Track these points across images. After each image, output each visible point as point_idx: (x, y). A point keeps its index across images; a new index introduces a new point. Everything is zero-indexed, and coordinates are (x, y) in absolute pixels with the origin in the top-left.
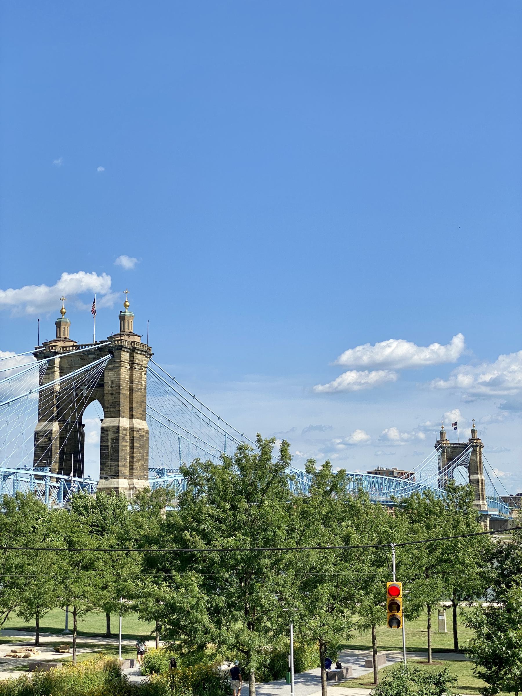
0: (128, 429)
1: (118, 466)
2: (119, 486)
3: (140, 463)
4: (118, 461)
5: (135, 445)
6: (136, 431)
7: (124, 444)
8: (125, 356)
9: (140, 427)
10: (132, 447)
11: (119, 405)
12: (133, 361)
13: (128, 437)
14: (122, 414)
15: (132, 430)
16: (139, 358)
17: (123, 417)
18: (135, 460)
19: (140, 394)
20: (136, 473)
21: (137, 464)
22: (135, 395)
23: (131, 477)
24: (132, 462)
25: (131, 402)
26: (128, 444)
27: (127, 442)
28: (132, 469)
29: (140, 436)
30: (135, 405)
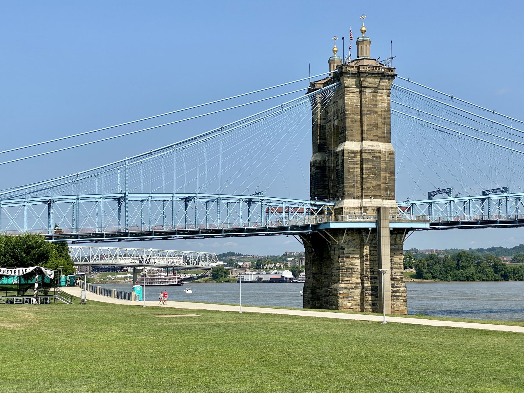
1: (344, 186)
2: (344, 206)
3: (374, 184)
4: (344, 183)
5: (364, 166)
7: (351, 166)
8: (350, 82)
9: (373, 148)
10: (362, 169)
11: (345, 130)
13: (358, 159)
14: (350, 138)
15: (362, 152)
16: (369, 81)
17: (352, 141)
18: (364, 180)
19: (373, 116)
20: (365, 193)
21: (369, 184)
22: (365, 118)
23: (362, 197)
24: (362, 183)
25: (362, 126)
26: (359, 166)
28: (362, 189)
29: (373, 157)
30: (364, 128)
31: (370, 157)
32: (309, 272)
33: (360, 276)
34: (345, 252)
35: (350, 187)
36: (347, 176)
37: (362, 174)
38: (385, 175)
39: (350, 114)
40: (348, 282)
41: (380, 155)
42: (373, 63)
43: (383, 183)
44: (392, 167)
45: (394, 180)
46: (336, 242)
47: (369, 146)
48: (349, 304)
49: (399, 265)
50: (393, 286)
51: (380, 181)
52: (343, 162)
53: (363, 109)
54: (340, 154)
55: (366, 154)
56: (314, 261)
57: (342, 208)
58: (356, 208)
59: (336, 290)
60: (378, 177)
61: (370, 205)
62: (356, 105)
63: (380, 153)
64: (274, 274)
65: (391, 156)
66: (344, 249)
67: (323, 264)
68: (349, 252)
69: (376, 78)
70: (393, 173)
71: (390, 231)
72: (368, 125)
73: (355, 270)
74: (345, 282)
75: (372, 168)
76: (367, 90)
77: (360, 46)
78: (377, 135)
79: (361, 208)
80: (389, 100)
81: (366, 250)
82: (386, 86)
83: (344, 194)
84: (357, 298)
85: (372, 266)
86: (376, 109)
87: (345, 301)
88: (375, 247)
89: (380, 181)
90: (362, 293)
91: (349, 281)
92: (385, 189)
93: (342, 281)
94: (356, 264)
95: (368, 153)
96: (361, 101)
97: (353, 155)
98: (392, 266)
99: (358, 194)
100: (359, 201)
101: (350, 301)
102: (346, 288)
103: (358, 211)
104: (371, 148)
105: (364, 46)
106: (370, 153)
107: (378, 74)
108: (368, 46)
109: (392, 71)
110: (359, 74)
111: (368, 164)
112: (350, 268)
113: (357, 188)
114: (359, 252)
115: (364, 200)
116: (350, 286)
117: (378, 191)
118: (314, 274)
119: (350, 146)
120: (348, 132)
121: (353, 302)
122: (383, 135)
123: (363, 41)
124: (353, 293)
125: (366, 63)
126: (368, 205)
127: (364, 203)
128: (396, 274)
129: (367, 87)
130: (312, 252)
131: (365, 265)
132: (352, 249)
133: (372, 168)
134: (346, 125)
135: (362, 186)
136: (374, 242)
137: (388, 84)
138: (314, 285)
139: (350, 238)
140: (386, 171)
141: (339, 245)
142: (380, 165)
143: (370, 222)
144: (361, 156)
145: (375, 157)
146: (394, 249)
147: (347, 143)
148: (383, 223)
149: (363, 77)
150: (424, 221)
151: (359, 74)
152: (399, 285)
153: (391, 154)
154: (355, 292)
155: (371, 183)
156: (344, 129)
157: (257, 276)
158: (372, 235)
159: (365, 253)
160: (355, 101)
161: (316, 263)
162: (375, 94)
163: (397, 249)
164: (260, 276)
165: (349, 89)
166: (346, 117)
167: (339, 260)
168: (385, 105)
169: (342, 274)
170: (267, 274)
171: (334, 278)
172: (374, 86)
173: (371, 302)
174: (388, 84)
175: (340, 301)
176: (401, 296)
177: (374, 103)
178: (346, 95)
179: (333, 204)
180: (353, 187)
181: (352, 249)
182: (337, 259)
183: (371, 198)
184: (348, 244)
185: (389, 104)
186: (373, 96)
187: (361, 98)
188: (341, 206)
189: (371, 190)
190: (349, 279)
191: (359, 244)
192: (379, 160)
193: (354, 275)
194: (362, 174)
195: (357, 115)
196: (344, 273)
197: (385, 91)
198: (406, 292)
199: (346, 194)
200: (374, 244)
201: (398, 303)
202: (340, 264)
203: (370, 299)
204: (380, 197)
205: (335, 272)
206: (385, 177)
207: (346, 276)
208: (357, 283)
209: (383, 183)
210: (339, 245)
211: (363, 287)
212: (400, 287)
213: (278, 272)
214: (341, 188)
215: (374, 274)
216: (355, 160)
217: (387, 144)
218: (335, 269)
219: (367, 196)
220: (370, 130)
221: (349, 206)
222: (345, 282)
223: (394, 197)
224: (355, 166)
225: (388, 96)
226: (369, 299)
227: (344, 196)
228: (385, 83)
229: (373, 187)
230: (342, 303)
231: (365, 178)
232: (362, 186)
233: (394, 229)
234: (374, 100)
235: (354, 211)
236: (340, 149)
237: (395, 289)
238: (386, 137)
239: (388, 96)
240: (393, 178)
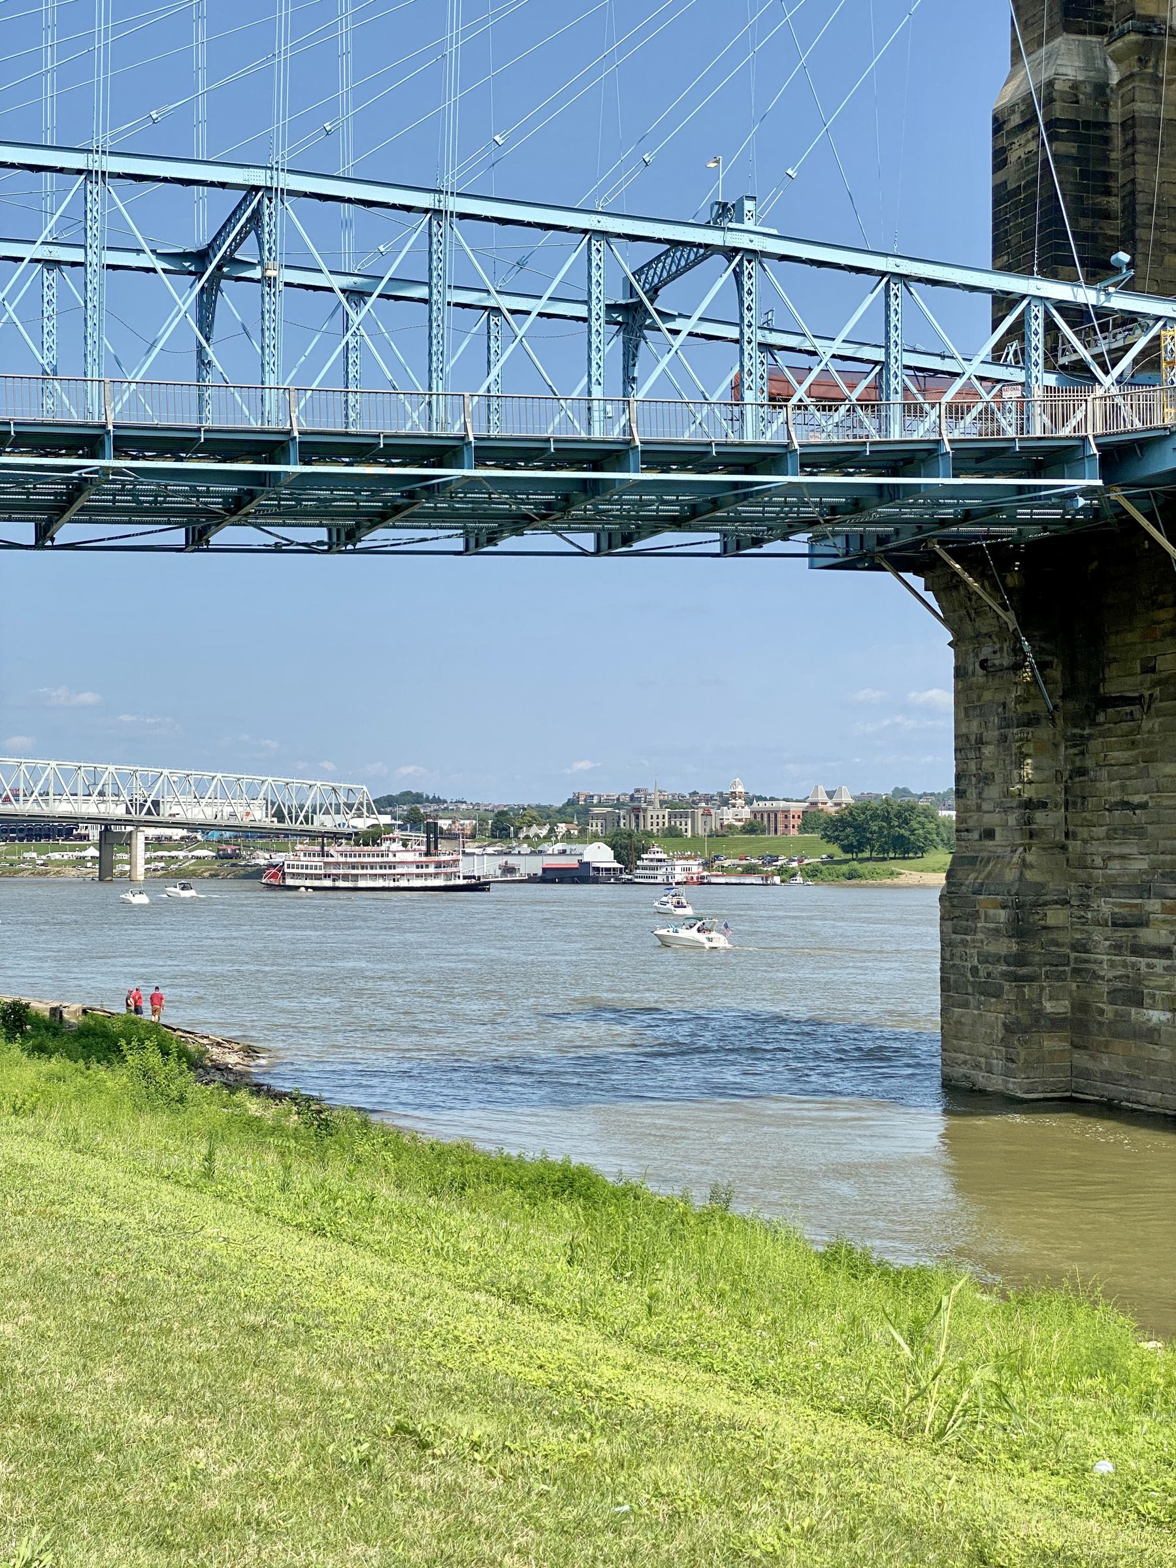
32: (993, 792)
56: (1031, 721)
64: (555, 856)
67: (1095, 745)
118: (1029, 805)
130: (1017, 667)
157: (502, 860)
161: (1044, 732)
164: (512, 861)
170: (533, 853)
213: (568, 847)
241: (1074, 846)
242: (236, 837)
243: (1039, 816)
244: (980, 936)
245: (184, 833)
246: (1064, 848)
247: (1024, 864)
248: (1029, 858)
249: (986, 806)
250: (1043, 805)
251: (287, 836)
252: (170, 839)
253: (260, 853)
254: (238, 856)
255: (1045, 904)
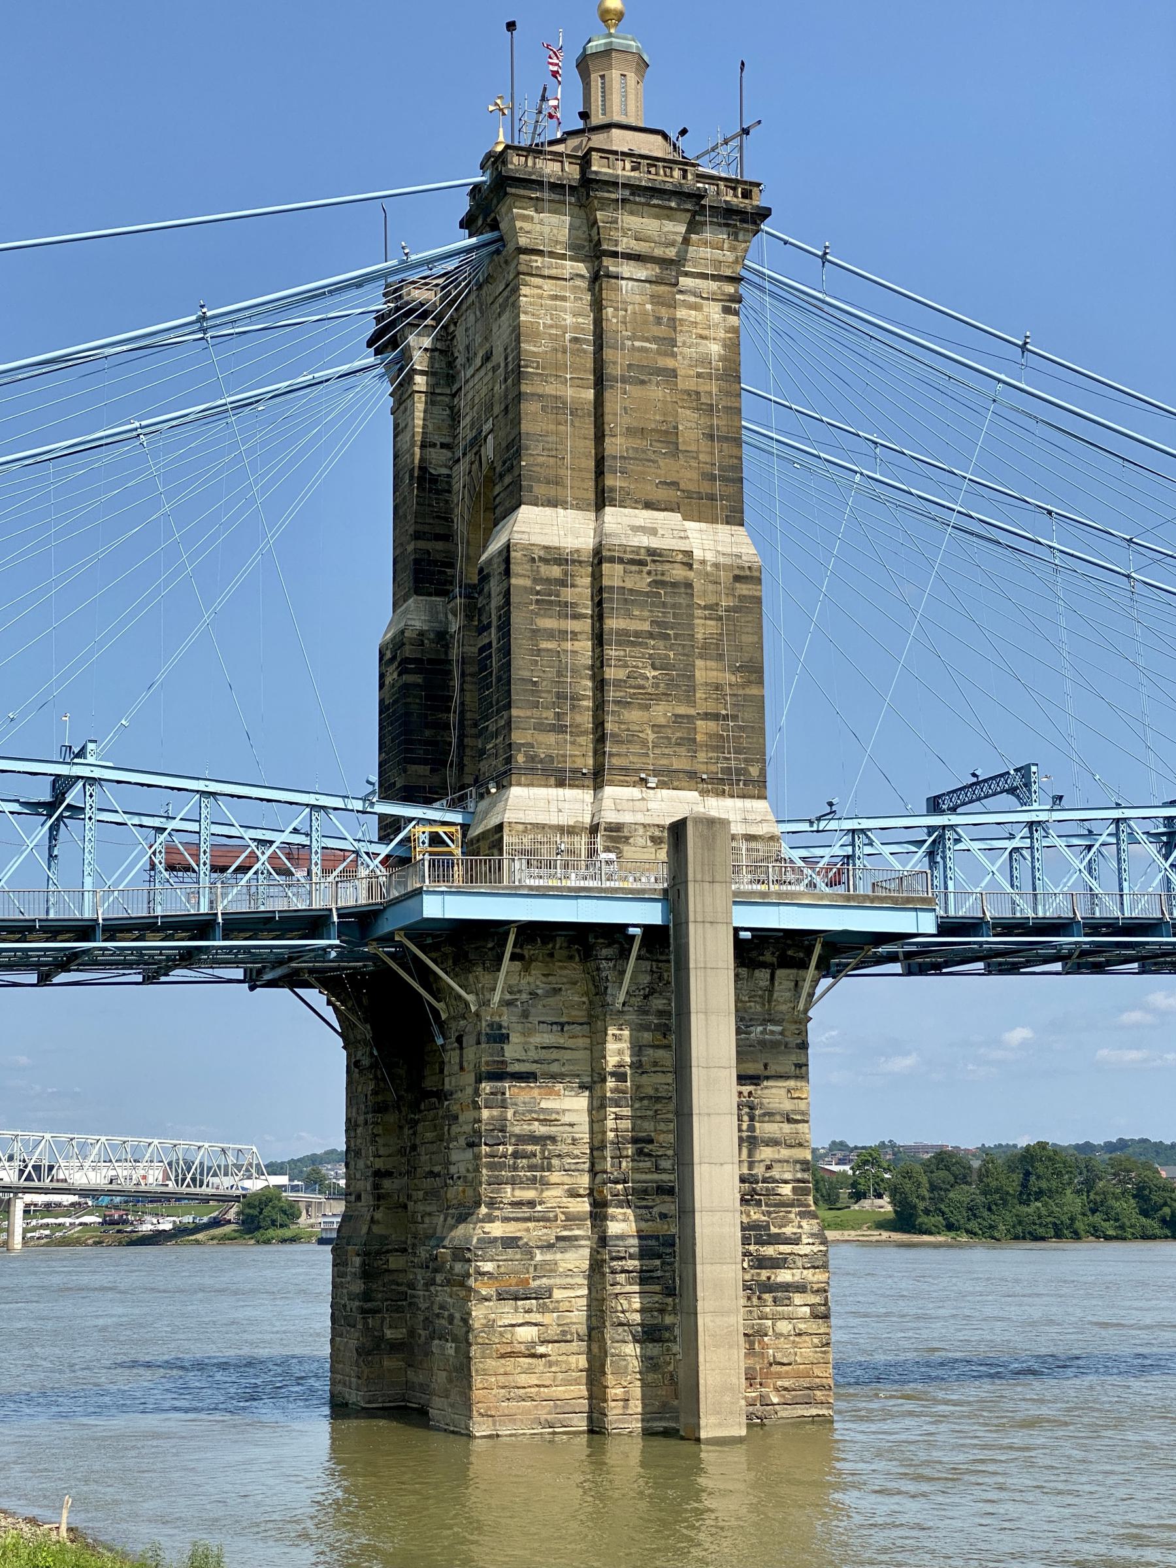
0: (586, 556)
2: (509, 817)
3: (661, 712)
4: (508, 706)
5: (613, 623)
6: (611, 560)
9: (655, 543)
10: (599, 639)
11: (518, 455)
12: (599, 243)
13: (580, 592)
14: (540, 490)
15: (599, 557)
16: (634, 228)
17: (553, 503)
18: (611, 694)
19: (657, 392)
21: (634, 715)
22: (615, 401)
23: (598, 779)
24: (599, 708)
25: (600, 437)
26: (585, 626)
27: (576, 617)
28: (600, 738)
30: (615, 445)
31: (642, 582)
33: (585, 1180)
34: (511, 1051)
35: (540, 727)
36: (526, 674)
37: (599, 663)
38: (714, 676)
39: (544, 378)
40: (526, 1211)
41: (691, 574)
42: (653, 146)
43: (707, 716)
44: (747, 639)
45: (759, 704)
46: (467, 1004)
47: (636, 529)
48: (527, 1334)
49: (787, 1128)
50: (754, 1233)
51: (690, 701)
52: (508, 603)
53: (608, 354)
54: (497, 568)
55: (619, 568)
57: (500, 828)
58: (571, 831)
59: (461, 1254)
60: (680, 684)
61: (640, 818)
62: (575, 340)
63: (690, 566)
65: (744, 589)
66: (504, 1038)
68: (533, 1054)
69: (667, 213)
70: (753, 671)
71: (739, 944)
72: (630, 432)
73: (562, 1148)
74: (509, 1211)
75: (651, 635)
76: (626, 269)
77: (595, 77)
78: (675, 484)
79: (594, 829)
80: (735, 330)
81: (617, 1049)
82: (718, 263)
83: (508, 760)
84: (573, 1298)
85: (648, 1126)
86: (670, 363)
87: (507, 1314)
88: (665, 1030)
89: (690, 701)
90: (596, 1269)
91: (531, 1204)
92: (718, 744)
93: (491, 1204)
94: (566, 1119)
95: (632, 562)
96: (598, 322)
97: (556, 571)
98: (751, 1128)
99: (579, 762)
100: (587, 795)
101: (536, 1317)
102: (510, 1242)
103: (581, 843)
104: (644, 541)
105: (615, 74)
106: (642, 563)
107: (678, 194)
108: (632, 77)
109: (746, 195)
110: (585, 191)
111: (630, 616)
112: (533, 1139)
113: (577, 731)
114: (583, 1055)
115: (608, 791)
116: (534, 1233)
117: (682, 751)
118: (378, 1174)
119: (545, 527)
120: (533, 459)
121: (547, 1318)
122: (706, 487)
123: (607, 53)
124: (548, 1269)
125: (620, 140)
126: (626, 818)
127: (607, 803)
128: (775, 1173)
129: (629, 257)
131: (610, 1124)
132: (548, 1039)
133: (651, 635)
134: (525, 427)
135: (599, 725)
136: (658, 1003)
137: (730, 256)
138: (376, 1229)
139: (535, 979)
140: (720, 657)
141: (477, 1015)
142: (691, 626)
143: (638, 896)
144: (597, 576)
145: (662, 584)
146: (763, 1043)
147: (526, 513)
148: (701, 900)
149: (605, 204)
150: (909, 900)
151: (585, 191)
152: (788, 1230)
153: (745, 576)
154: (563, 1267)
155: (647, 708)
156: (513, 449)
158: (646, 965)
159: (612, 1061)
160: (569, 320)
162: (662, 289)
163: (774, 1045)
165: (538, 261)
166: (526, 388)
167: (477, 1092)
168: (715, 349)
169: (491, 1167)
171: (454, 1192)
172: (658, 252)
173: (637, 1318)
174: (730, 256)
175: (479, 1313)
176: (801, 1288)
177: (662, 331)
178: (524, 290)
179: (457, 818)
180: (562, 729)
181: (548, 1039)
182: (469, 1091)
183: (644, 781)
184: (525, 1015)
185: (733, 346)
186: (656, 299)
187: (597, 306)
188: (493, 822)
189: (644, 743)
190: (530, 1194)
191: (580, 1014)
192: (682, 601)
193: (555, 1177)
194: (599, 663)
195: (578, 383)
196: (502, 1166)
197: (713, 285)
198: (825, 1267)
199: (521, 758)
200: (660, 1013)
201: (784, 1327)
202: (485, 1114)
203: (636, 1303)
204: (692, 779)
205: (460, 1158)
206: (718, 687)
207: (513, 1182)
208: (570, 1218)
209: (707, 716)
210: (477, 1015)
211: (603, 1241)
212: (796, 1241)
214: (496, 734)
215: (658, 1169)
216: (568, 594)
217: (723, 531)
218: (462, 1141)
219: (625, 771)
220: (640, 457)
221: (531, 818)
222: (509, 1211)
223: (761, 783)
224: (571, 625)
225: (727, 310)
226: (630, 1303)
227: (507, 773)
228: (711, 249)
229: (656, 727)
230: (490, 1325)
231: (618, 683)
232: (599, 725)
233: (762, 937)
234: (658, 320)
235: (563, 842)
236: (495, 546)
237: (769, 1251)
238: (722, 499)
239: (727, 310)
240: (753, 691)
241: (411, 1205)
242: (126, 1202)
243: (387, 1184)
244: (349, 1278)
245: (75, 1199)
246: (405, 1207)
247: (372, 1221)
248: (378, 1216)
249: (358, 1176)
250: (388, 1174)
251: (178, 1200)
252: (59, 1205)
253: (147, 1218)
254: (126, 1222)
255: (388, 1252)
